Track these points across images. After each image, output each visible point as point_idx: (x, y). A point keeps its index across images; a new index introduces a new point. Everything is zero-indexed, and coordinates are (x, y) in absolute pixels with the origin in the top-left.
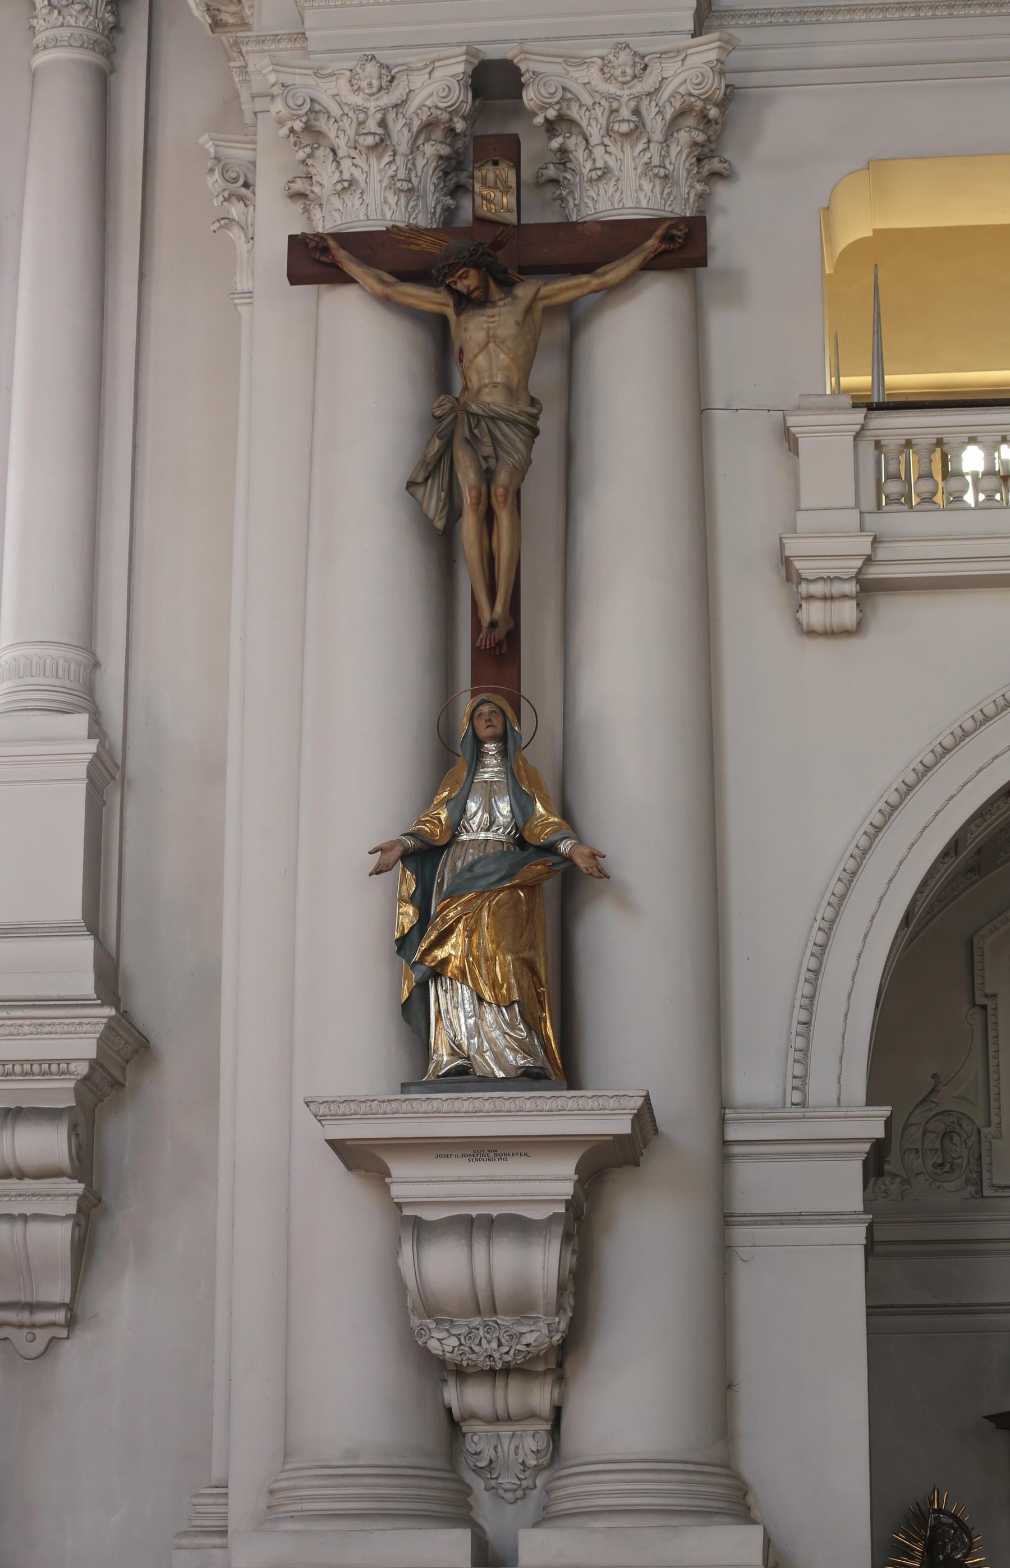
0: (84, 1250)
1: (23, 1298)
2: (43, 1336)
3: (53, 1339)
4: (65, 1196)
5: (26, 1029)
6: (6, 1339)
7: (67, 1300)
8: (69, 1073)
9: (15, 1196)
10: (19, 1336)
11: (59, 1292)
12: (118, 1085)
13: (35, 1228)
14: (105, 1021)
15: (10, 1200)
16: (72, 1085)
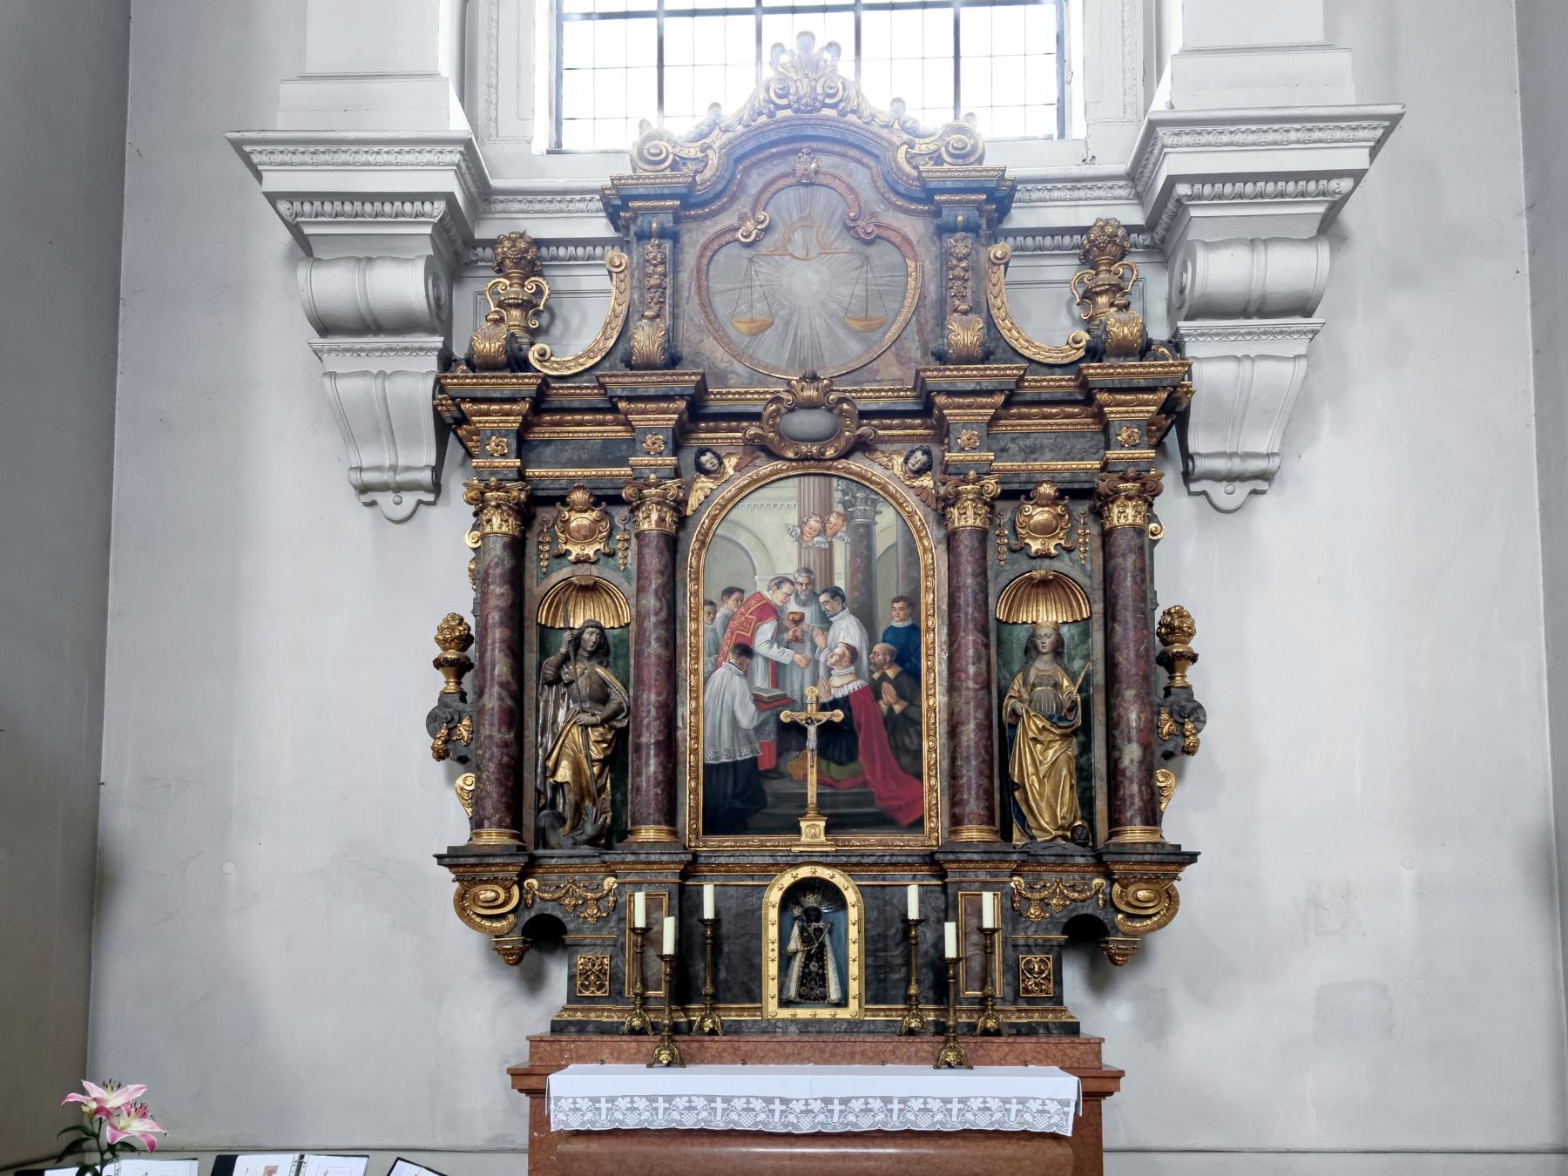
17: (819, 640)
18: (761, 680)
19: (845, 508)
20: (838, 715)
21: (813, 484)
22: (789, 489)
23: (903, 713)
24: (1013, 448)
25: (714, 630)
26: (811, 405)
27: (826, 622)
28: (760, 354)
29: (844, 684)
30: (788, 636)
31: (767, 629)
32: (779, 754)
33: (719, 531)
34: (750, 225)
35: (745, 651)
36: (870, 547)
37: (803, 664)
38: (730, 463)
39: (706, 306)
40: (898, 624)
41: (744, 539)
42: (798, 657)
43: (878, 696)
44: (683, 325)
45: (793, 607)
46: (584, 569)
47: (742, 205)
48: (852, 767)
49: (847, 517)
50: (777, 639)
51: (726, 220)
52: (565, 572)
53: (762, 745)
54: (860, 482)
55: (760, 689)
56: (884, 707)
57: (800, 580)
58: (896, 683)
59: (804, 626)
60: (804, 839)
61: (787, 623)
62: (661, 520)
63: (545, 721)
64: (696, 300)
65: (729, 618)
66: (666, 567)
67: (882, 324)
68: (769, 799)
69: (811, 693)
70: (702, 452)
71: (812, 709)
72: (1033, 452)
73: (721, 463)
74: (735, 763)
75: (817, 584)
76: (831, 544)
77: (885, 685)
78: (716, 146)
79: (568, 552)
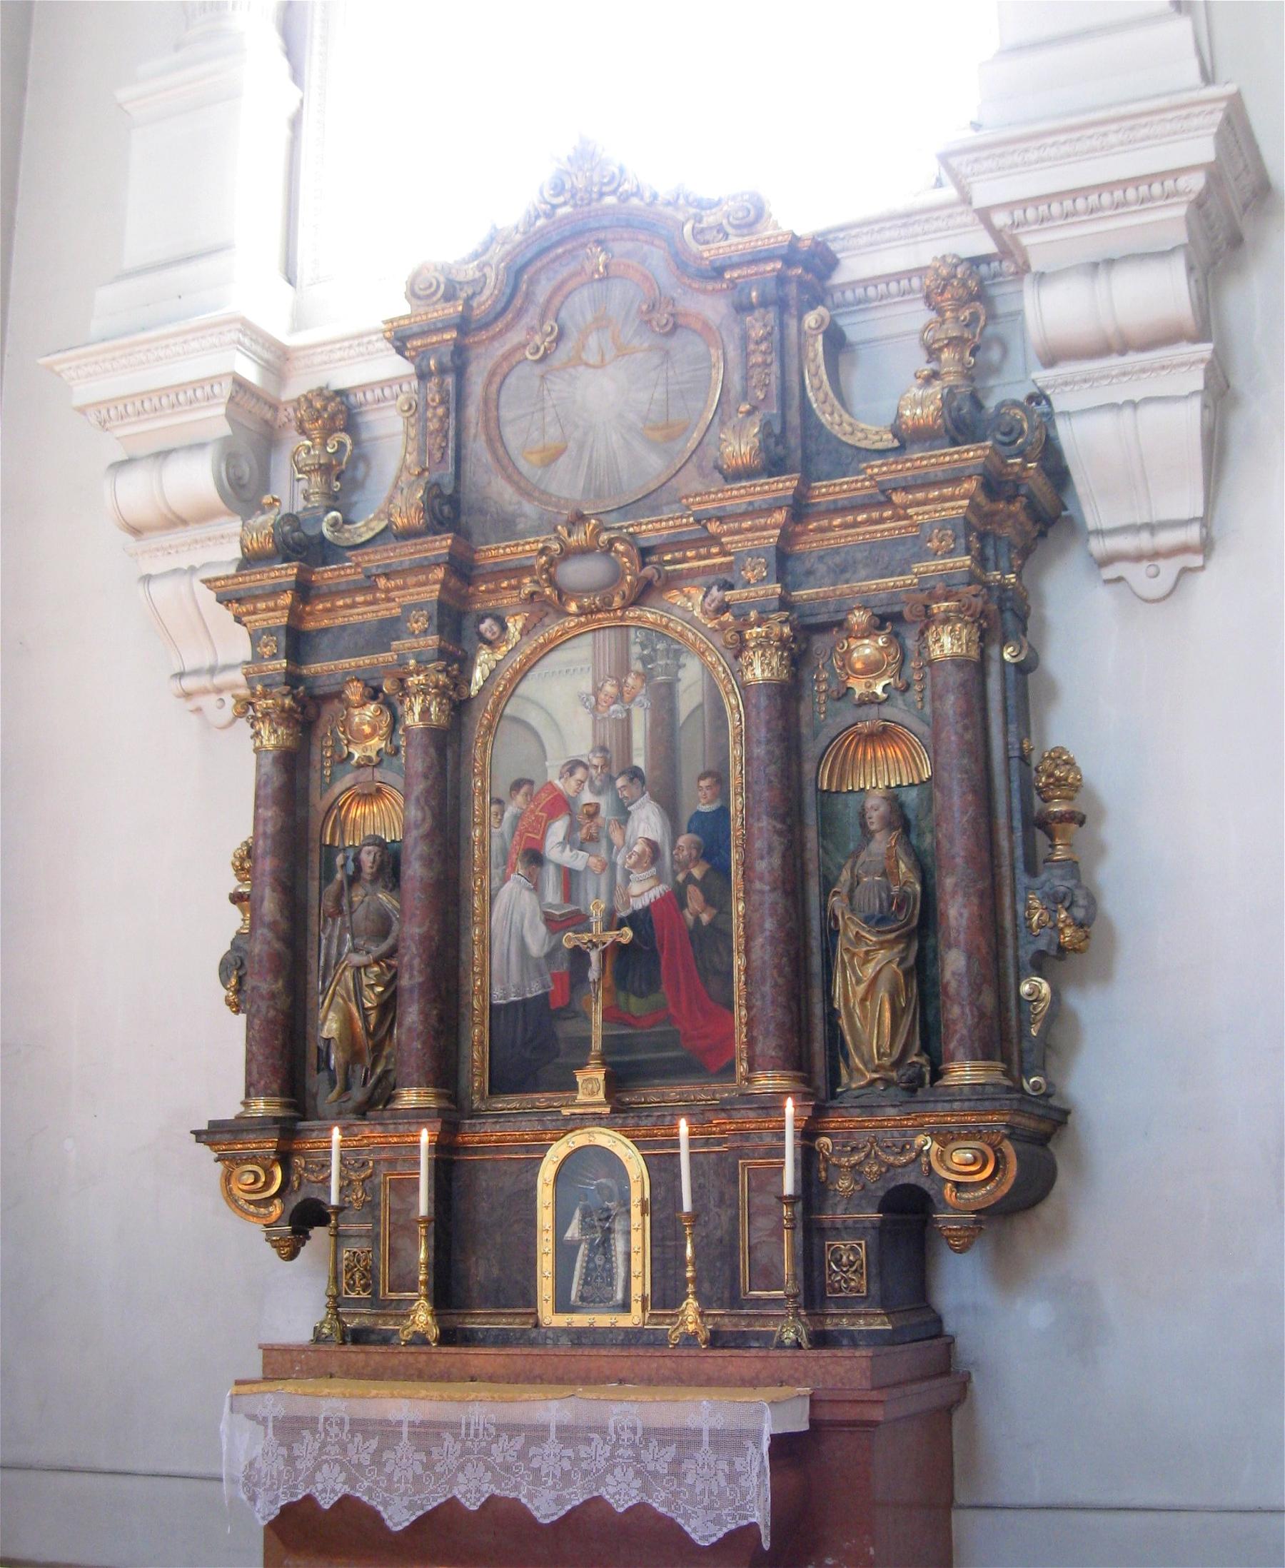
0: (1216, 450)
1: (1141, 518)
2: (1169, 569)
3: (1185, 571)
4: (1185, 371)
5: (1113, 139)
6: (1120, 579)
7: (1200, 513)
8: (1176, 193)
9: (1117, 376)
10: (1136, 574)
11: (1189, 503)
12: (1236, 241)
13: (1149, 414)
14: (1223, 105)
15: (1109, 384)
16: (1181, 211)
17: (616, 837)
18: (552, 894)
19: (644, 664)
20: (627, 935)
21: (608, 641)
22: (580, 653)
23: (712, 924)
24: (821, 569)
25: (502, 835)
26: (583, 551)
27: (623, 813)
28: (553, 488)
29: (643, 891)
30: (581, 835)
31: (558, 829)
32: (573, 987)
33: (508, 711)
34: (537, 339)
35: (535, 857)
36: (672, 711)
37: (598, 870)
38: (515, 626)
39: (495, 441)
40: (705, 808)
41: (534, 718)
42: (593, 860)
43: (683, 904)
44: (468, 467)
45: (587, 797)
46: (366, 774)
47: (530, 318)
48: (653, 998)
49: (646, 677)
50: (569, 840)
51: (516, 337)
52: (347, 780)
53: (554, 976)
54: (658, 633)
55: (551, 906)
56: (690, 918)
57: (596, 761)
58: (703, 885)
59: (599, 820)
60: (581, 1097)
61: (580, 818)
62: (425, 712)
63: (327, 961)
64: (483, 438)
65: (518, 818)
66: (430, 768)
67: (685, 429)
68: (562, 1046)
69: (596, 910)
70: (482, 620)
71: (597, 927)
72: (843, 571)
73: (504, 628)
74: (525, 1002)
75: (614, 765)
76: (628, 712)
77: (691, 888)
78: (494, 262)
79: (350, 755)
